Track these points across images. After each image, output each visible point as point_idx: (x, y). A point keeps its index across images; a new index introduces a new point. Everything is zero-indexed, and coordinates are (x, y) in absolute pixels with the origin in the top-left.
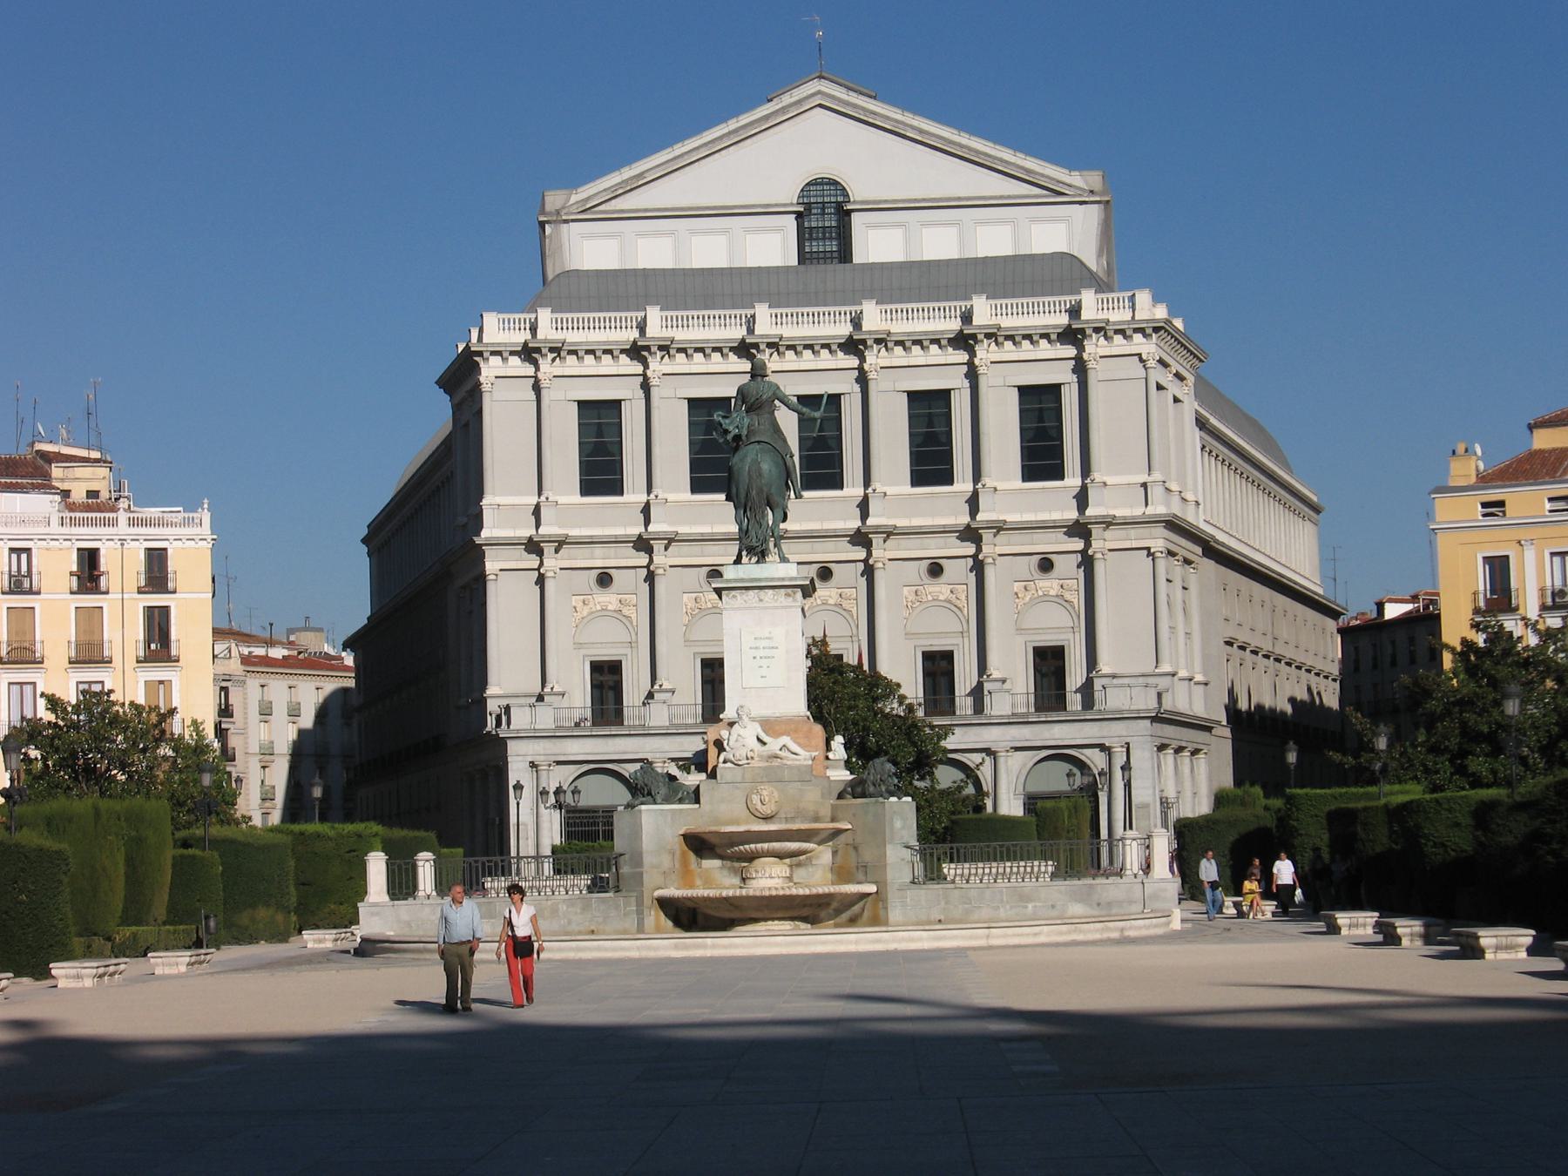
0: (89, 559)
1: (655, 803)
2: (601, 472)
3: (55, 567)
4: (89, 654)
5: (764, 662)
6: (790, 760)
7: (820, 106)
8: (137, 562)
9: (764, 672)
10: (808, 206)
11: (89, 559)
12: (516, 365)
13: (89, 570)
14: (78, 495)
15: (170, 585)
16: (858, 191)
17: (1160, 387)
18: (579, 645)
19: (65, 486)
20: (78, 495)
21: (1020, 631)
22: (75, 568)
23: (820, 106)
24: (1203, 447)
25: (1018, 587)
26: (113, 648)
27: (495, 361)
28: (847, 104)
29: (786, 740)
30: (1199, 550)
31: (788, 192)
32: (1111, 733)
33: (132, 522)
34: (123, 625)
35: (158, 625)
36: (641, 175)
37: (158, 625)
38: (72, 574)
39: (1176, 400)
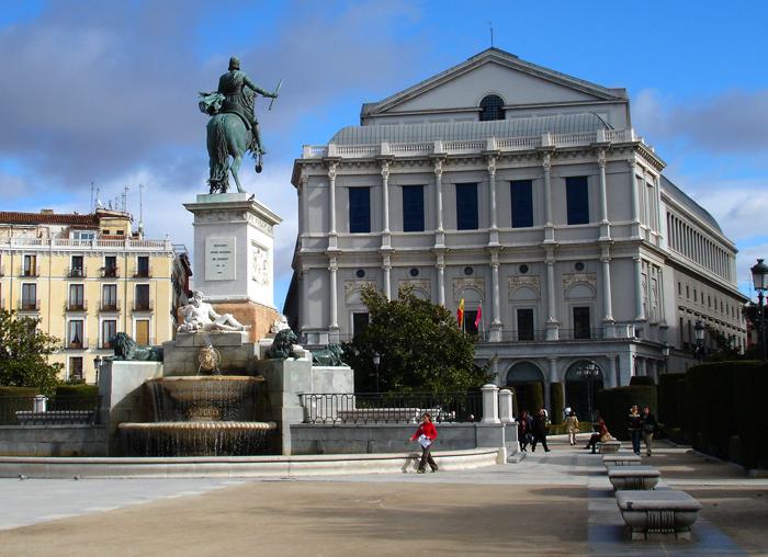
0: (111, 261)
1: (124, 359)
2: (360, 218)
3: (94, 265)
4: (110, 307)
5: (221, 262)
6: (228, 330)
7: (490, 62)
8: (133, 263)
9: (220, 269)
10: (485, 108)
11: (111, 261)
12: (318, 172)
13: (110, 270)
14: (113, 232)
15: (150, 275)
16: (509, 100)
17: (638, 177)
18: (348, 305)
19: (107, 229)
20: (113, 232)
21: (567, 299)
22: (104, 266)
23: (490, 62)
24: (668, 214)
25: (566, 277)
26: (121, 305)
27: (308, 168)
28: (503, 60)
29: (230, 317)
30: (663, 261)
31: (474, 101)
32: (610, 352)
33: (132, 245)
34: (126, 294)
35: (143, 292)
36: (407, 96)
37: (143, 292)
38: (102, 269)
39: (649, 185)
